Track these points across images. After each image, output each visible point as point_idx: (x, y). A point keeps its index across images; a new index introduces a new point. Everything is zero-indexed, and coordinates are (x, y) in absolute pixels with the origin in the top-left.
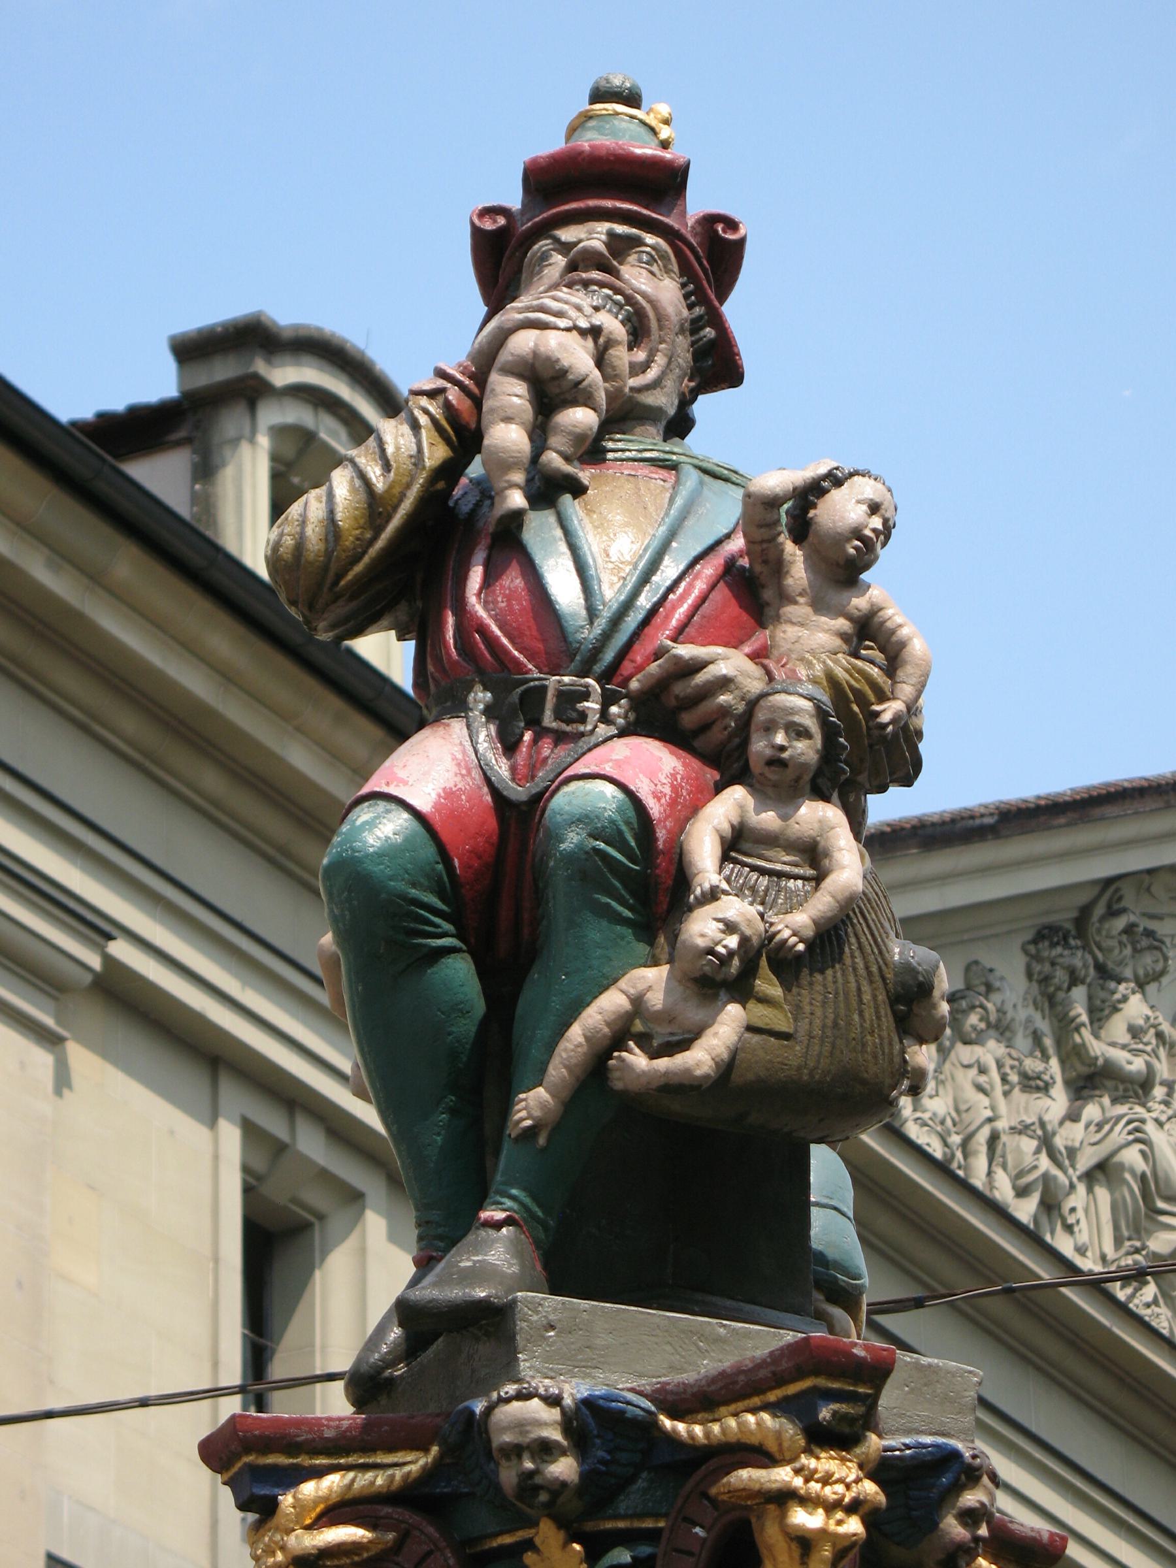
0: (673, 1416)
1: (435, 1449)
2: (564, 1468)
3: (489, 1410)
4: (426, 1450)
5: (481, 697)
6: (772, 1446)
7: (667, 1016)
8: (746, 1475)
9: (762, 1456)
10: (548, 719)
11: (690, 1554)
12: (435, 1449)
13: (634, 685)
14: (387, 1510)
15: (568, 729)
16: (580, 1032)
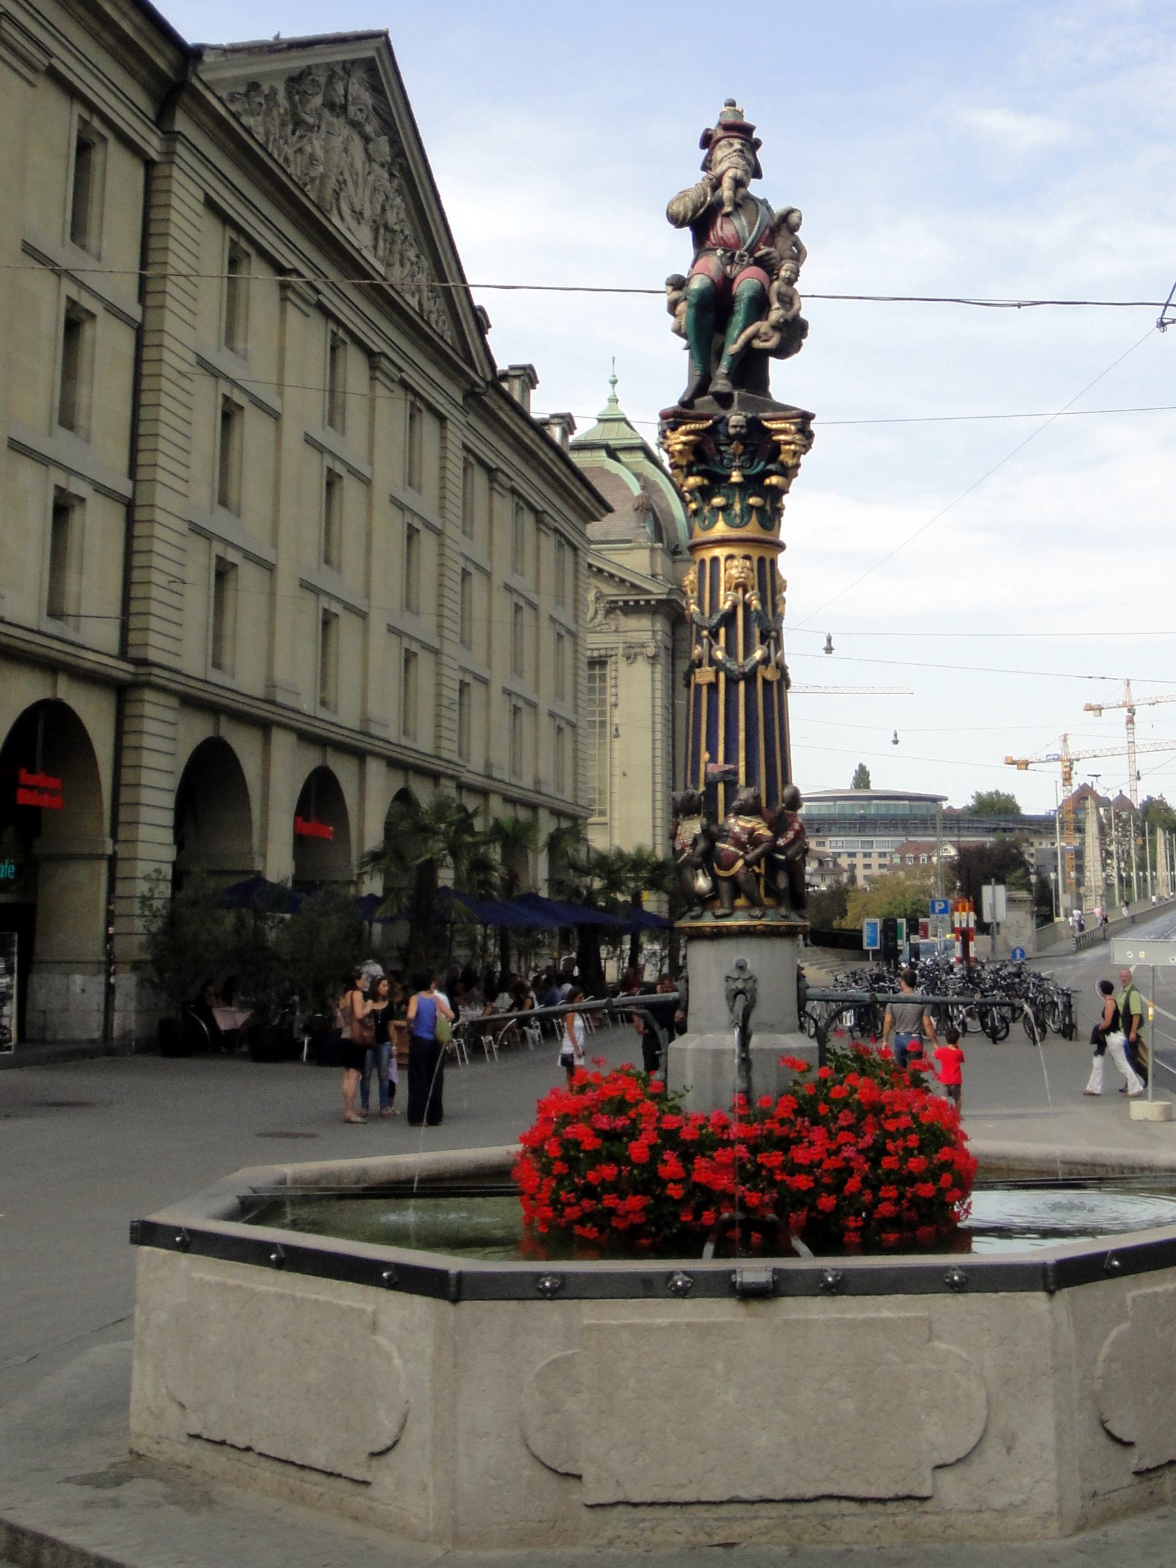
2: (744, 431)
5: (719, 252)
7: (765, 334)
8: (782, 437)
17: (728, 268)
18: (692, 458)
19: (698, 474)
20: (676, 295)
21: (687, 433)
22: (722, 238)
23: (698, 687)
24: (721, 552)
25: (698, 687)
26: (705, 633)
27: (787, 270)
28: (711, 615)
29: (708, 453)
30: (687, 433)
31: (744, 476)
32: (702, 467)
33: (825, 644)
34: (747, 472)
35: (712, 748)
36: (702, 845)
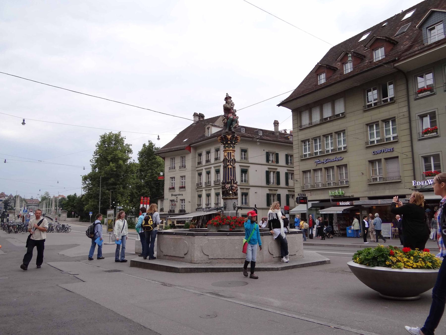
20: (224, 118)
21: (231, 136)
23: (228, 168)
24: (231, 152)
25: (229, 168)
26: (230, 161)
28: (230, 159)
30: (231, 136)
33: (4, 161)
35: (231, 175)
36: (230, 188)
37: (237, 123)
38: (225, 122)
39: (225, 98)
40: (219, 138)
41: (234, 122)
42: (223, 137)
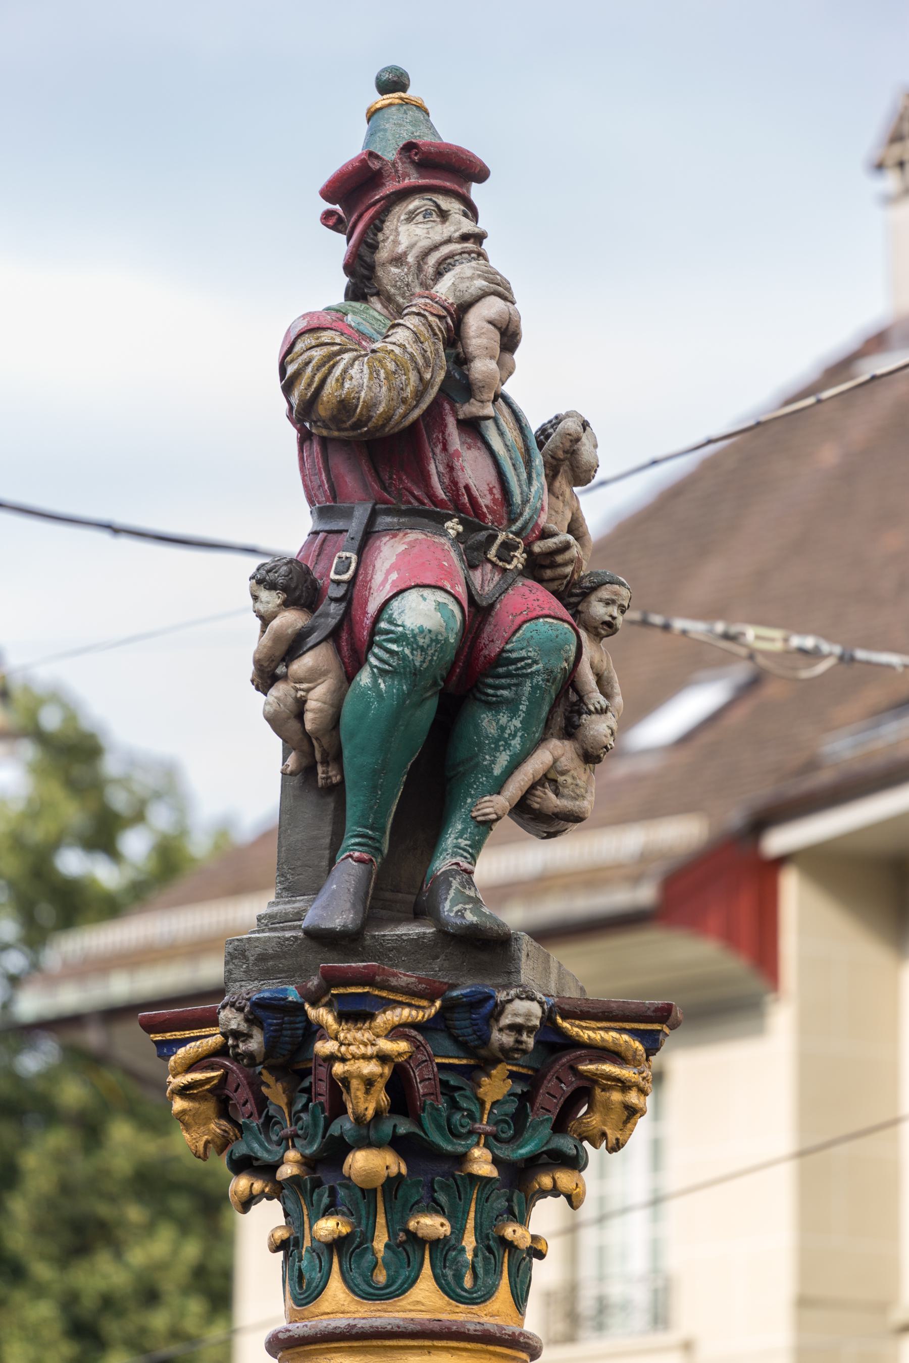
0: (564, 1018)
1: (438, 1004)
3: (510, 1001)
4: (433, 1002)
5: (453, 527)
6: (629, 1055)
8: (608, 1068)
9: (615, 1055)
10: (492, 554)
11: (555, 1097)
12: (438, 1004)
13: (538, 547)
14: (414, 1033)
15: (501, 564)
16: (531, 771)
17: (477, 576)
18: (384, 1098)
19: (376, 1145)
21: (396, 1032)
22: (467, 488)
27: (608, 603)
29: (421, 1088)
30: (396, 1032)
31: (496, 1161)
32: (404, 1127)
34: (506, 1152)
37: (570, 731)
38: (301, 703)
39: (328, 194)
40: (191, 1066)
41: (494, 706)
42: (255, 1044)
